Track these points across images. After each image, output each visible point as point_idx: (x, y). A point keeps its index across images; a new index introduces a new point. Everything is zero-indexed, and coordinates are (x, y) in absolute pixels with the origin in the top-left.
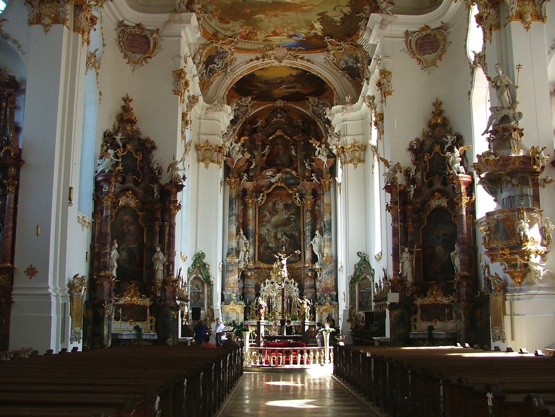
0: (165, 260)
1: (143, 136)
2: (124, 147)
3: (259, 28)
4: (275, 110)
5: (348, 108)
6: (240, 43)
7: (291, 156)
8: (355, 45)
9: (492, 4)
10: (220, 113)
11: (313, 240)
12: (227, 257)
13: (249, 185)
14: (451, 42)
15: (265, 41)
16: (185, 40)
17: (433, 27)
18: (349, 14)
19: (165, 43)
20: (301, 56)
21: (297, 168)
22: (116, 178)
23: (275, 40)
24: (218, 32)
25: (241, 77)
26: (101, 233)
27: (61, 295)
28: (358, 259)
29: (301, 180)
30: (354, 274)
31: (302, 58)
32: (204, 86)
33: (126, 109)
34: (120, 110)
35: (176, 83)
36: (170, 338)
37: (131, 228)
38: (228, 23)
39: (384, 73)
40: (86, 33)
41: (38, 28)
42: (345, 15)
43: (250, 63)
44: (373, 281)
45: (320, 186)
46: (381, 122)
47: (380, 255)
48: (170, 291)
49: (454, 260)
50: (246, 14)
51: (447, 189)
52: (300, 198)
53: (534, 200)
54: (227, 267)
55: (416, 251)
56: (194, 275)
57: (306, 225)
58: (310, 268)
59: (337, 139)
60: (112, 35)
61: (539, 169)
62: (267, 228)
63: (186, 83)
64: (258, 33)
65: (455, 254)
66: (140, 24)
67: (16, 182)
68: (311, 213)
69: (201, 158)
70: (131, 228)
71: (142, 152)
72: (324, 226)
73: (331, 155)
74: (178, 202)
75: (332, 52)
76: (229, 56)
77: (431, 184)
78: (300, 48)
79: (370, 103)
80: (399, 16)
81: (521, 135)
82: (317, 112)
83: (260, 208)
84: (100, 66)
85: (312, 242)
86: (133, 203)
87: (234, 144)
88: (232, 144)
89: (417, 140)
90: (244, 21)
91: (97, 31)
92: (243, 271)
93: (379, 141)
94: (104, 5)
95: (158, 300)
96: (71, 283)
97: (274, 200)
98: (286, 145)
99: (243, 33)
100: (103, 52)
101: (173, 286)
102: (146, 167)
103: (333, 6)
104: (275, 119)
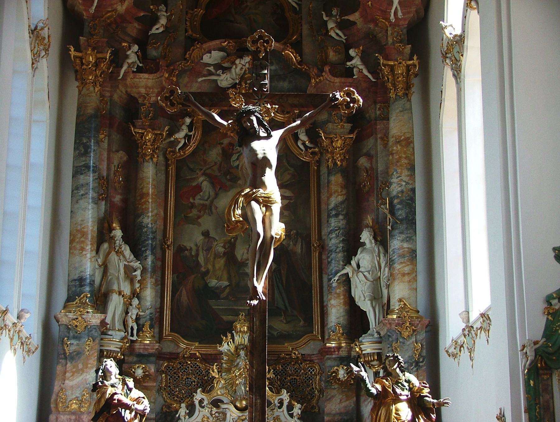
11: (353, 263)
52: (308, 133)
57: (329, 216)
58: (343, 353)
62: (204, 227)
68: (343, 177)
72: (392, 211)
83: (181, 164)
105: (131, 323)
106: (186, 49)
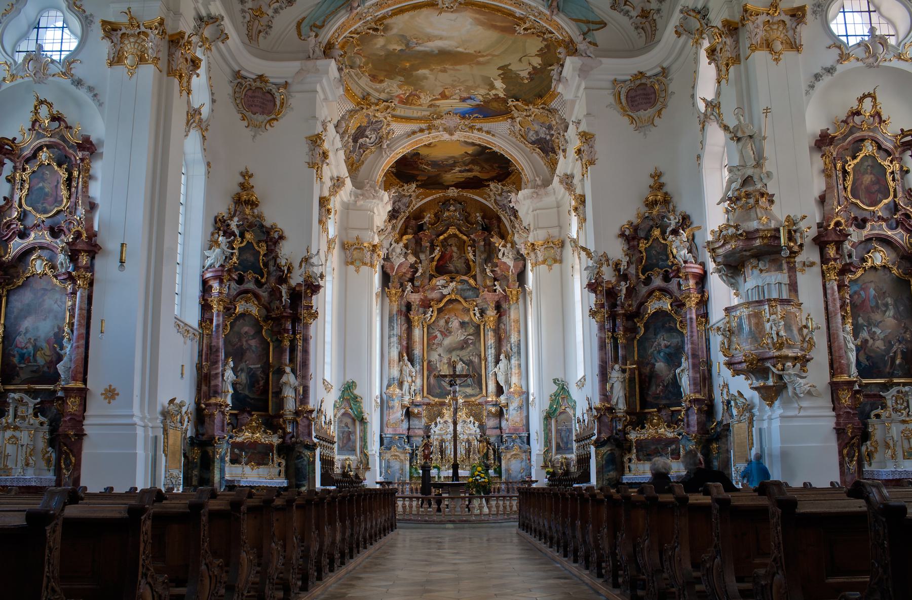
0: (297, 383)
1: (268, 223)
2: (242, 236)
3: (422, 89)
4: (446, 202)
5: (540, 193)
6: (399, 109)
7: (467, 262)
8: (547, 110)
9: (729, 30)
10: (374, 201)
12: (387, 389)
13: (415, 298)
14: (673, 93)
15: (430, 106)
16: (322, 97)
17: (648, 74)
18: (539, 67)
19: (296, 101)
20: (478, 126)
21: (475, 275)
22: (229, 275)
23: (445, 105)
24: (369, 94)
25: (400, 156)
26: (210, 347)
27: (150, 425)
28: (555, 388)
29: (481, 291)
30: (551, 406)
31: (480, 130)
32: (352, 166)
33: (242, 186)
34: (238, 189)
35: (311, 153)
36: (304, 486)
37: (253, 343)
38: (381, 81)
39: (586, 137)
40: (185, 80)
41: (119, 69)
42: (534, 68)
43: (413, 136)
44: (575, 416)
45: (506, 297)
46: (581, 207)
47: (583, 380)
48: (303, 424)
49: (681, 379)
50: (405, 69)
51: (670, 286)
53: (790, 290)
54: (388, 402)
55: (630, 369)
56: (342, 411)
59: (525, 235)
60: (226, 90)
61: (796, 249)
63: (324, 153)
64: (422, 95)
65: (682, 371)
66: (262, 75)
67: (89, 275)
69: (349, 260)
70: (253, 343)
71: (266, 242)
73: (520, 258)
74: (314, 308)
75: (518, 120)
76: (384, 127)
77: (647, 282)
78: (476, 115)
79: (567, 184)
80: (604, 60)
81: (771, 202)
82: (501, 203)
84: (209, 128)
85: (496, 370)
86: (254, 310)
87: (394, 245)
88: (391, 245)
89: (631, 224)
90: (402, 79)
91: (201, 76)
92: (408, 408)
93: (580, 232)
94: (213, 48)
95: (288, 437)
96: (166, 410)
97: (447, 317)
98: (462, 246)
99: (402, 96)
100: (213, 111)
101: (307, 418)
102: (271, 263)
103: (520, 55)
104: (446, 214)
105: (412, 393)
106: (430, 280)
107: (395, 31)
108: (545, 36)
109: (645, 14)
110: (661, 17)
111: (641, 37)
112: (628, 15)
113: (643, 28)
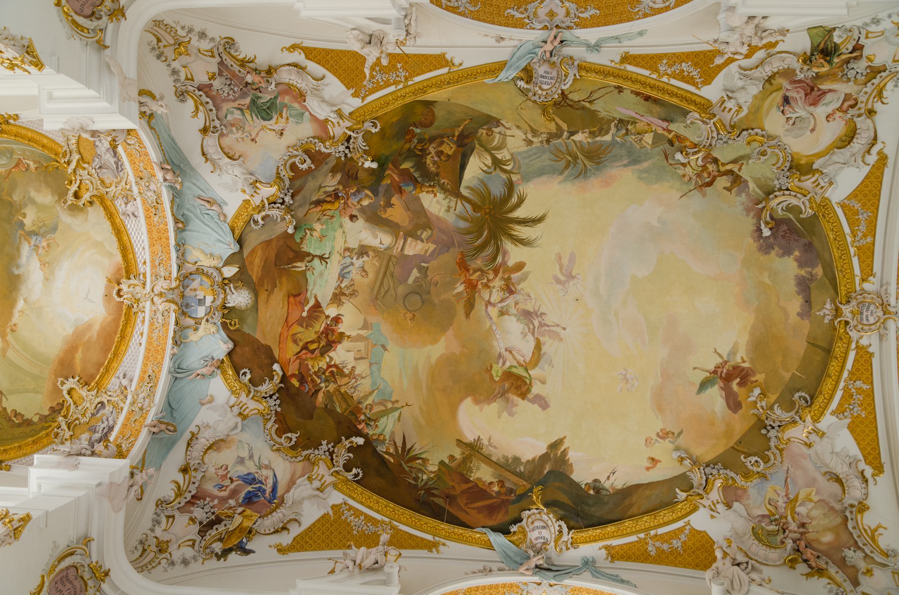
66: (124, 15)
80: (121, 515)
107: (66, 218)
108: (60, 419)
109: (162, 547)
110: (166, 571)
111: (133, 553)
112: (154, 526)
113: (144, 550)
